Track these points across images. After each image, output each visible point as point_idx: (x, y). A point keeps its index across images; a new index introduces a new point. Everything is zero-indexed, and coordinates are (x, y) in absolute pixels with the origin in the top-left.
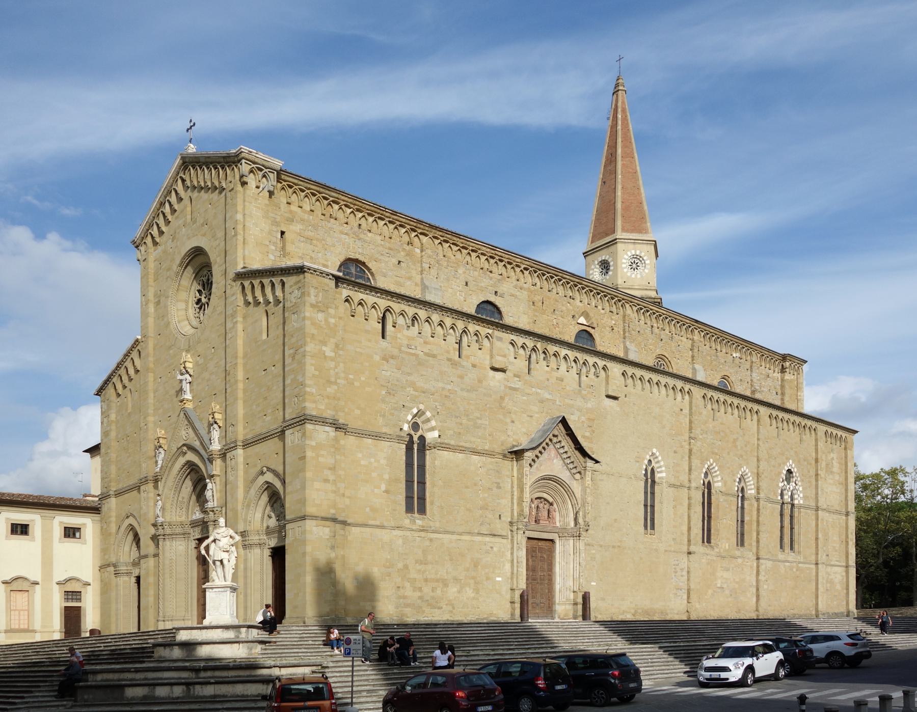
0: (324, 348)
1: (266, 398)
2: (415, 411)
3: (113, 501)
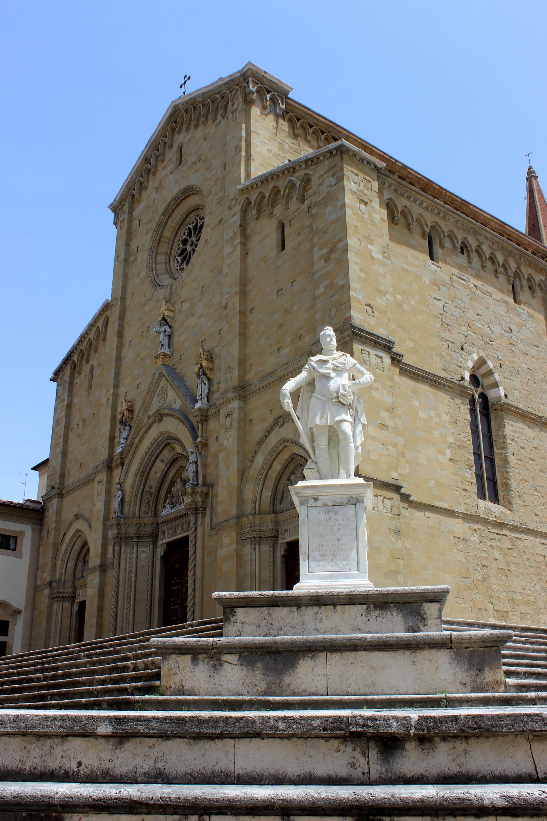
0: (371, 247)
1: (281, 326)
2: (475, 357)
3: (55, 501)
